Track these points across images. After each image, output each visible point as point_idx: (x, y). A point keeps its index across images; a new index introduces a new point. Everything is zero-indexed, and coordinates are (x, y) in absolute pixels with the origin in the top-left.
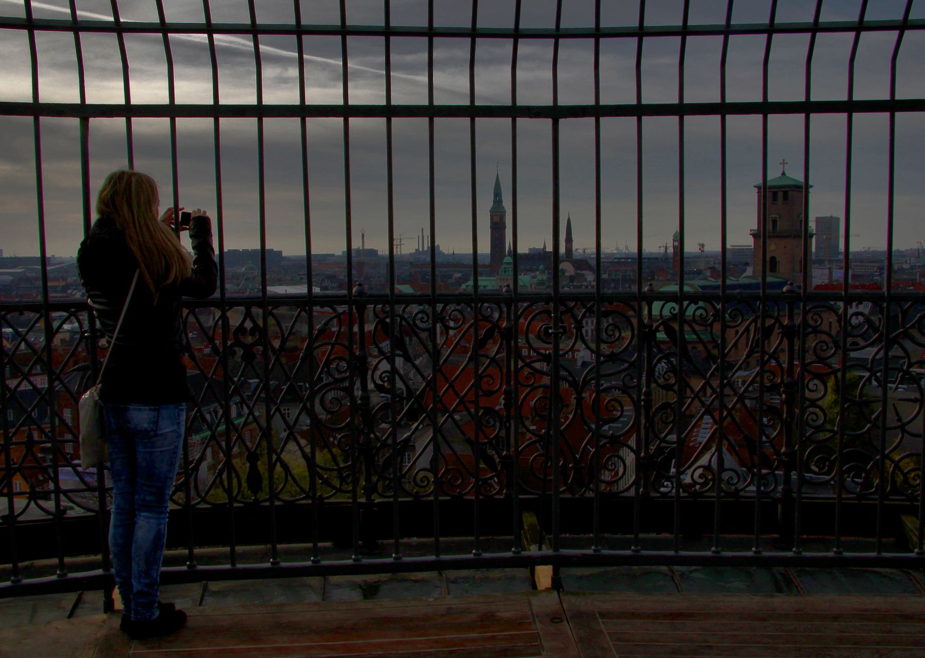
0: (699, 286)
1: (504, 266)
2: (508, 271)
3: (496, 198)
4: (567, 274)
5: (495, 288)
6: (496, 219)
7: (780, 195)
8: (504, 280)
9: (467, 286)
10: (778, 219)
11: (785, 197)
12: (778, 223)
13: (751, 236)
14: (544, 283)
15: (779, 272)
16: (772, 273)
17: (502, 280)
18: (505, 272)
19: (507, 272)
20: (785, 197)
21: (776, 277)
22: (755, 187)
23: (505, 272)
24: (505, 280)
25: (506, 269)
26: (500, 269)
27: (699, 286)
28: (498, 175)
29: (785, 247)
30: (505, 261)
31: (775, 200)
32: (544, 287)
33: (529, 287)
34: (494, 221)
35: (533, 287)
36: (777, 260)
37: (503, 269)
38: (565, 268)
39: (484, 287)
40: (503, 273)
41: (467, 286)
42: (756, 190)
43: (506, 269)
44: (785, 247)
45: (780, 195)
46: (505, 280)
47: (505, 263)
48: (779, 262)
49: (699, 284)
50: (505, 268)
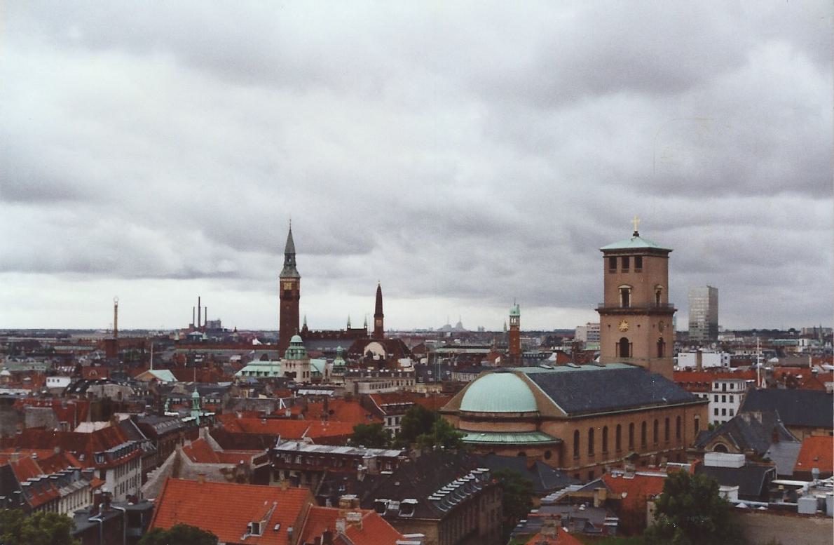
0: (527, 374)
1: (291, 347)
2: (297, 353)
3: (288, 260)
4: (376, 358)
5: (280, 375)
6: (288, 286)
7: (632, 261)
8: (291, 365)
9: (243, 372)
10: (629, 290)
11: (639, 264)
12: (630, 295)
13: (597, 312)
14: (342, 369)
15: (631, 357)
16: (623, 360)
17: (289, 366)
18: (292, 354)
19: (295, 356)
20: (639, 264)
21: (627, 364)
22: (602, 250)
23: (292, 354)
24: (293, 366)
25: (294, 351)
26: (286, 351)
27: (527, 374)
28: (290, 230)
29: (639, 326)
30: (292, 341)
31: (613, 268)
32: (342, 374)
33: (324, 374)
34: (285, 288)
35: (329, 374)
36: (630, 342)
37: (290, 351)
38: (372, 351)
39: (266, 373)
40: (290, 356)
41: (243, 372)
42: (603, 254)
43: (294, 351)
44: (639, 326)
45: (632, 261)
46: (293, 366)
47: (293, 343)
48: (632, 343)
49: (529, 372)
50: (292, 350)
